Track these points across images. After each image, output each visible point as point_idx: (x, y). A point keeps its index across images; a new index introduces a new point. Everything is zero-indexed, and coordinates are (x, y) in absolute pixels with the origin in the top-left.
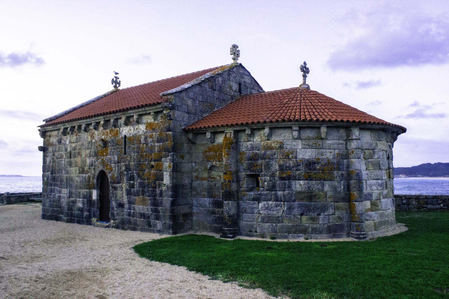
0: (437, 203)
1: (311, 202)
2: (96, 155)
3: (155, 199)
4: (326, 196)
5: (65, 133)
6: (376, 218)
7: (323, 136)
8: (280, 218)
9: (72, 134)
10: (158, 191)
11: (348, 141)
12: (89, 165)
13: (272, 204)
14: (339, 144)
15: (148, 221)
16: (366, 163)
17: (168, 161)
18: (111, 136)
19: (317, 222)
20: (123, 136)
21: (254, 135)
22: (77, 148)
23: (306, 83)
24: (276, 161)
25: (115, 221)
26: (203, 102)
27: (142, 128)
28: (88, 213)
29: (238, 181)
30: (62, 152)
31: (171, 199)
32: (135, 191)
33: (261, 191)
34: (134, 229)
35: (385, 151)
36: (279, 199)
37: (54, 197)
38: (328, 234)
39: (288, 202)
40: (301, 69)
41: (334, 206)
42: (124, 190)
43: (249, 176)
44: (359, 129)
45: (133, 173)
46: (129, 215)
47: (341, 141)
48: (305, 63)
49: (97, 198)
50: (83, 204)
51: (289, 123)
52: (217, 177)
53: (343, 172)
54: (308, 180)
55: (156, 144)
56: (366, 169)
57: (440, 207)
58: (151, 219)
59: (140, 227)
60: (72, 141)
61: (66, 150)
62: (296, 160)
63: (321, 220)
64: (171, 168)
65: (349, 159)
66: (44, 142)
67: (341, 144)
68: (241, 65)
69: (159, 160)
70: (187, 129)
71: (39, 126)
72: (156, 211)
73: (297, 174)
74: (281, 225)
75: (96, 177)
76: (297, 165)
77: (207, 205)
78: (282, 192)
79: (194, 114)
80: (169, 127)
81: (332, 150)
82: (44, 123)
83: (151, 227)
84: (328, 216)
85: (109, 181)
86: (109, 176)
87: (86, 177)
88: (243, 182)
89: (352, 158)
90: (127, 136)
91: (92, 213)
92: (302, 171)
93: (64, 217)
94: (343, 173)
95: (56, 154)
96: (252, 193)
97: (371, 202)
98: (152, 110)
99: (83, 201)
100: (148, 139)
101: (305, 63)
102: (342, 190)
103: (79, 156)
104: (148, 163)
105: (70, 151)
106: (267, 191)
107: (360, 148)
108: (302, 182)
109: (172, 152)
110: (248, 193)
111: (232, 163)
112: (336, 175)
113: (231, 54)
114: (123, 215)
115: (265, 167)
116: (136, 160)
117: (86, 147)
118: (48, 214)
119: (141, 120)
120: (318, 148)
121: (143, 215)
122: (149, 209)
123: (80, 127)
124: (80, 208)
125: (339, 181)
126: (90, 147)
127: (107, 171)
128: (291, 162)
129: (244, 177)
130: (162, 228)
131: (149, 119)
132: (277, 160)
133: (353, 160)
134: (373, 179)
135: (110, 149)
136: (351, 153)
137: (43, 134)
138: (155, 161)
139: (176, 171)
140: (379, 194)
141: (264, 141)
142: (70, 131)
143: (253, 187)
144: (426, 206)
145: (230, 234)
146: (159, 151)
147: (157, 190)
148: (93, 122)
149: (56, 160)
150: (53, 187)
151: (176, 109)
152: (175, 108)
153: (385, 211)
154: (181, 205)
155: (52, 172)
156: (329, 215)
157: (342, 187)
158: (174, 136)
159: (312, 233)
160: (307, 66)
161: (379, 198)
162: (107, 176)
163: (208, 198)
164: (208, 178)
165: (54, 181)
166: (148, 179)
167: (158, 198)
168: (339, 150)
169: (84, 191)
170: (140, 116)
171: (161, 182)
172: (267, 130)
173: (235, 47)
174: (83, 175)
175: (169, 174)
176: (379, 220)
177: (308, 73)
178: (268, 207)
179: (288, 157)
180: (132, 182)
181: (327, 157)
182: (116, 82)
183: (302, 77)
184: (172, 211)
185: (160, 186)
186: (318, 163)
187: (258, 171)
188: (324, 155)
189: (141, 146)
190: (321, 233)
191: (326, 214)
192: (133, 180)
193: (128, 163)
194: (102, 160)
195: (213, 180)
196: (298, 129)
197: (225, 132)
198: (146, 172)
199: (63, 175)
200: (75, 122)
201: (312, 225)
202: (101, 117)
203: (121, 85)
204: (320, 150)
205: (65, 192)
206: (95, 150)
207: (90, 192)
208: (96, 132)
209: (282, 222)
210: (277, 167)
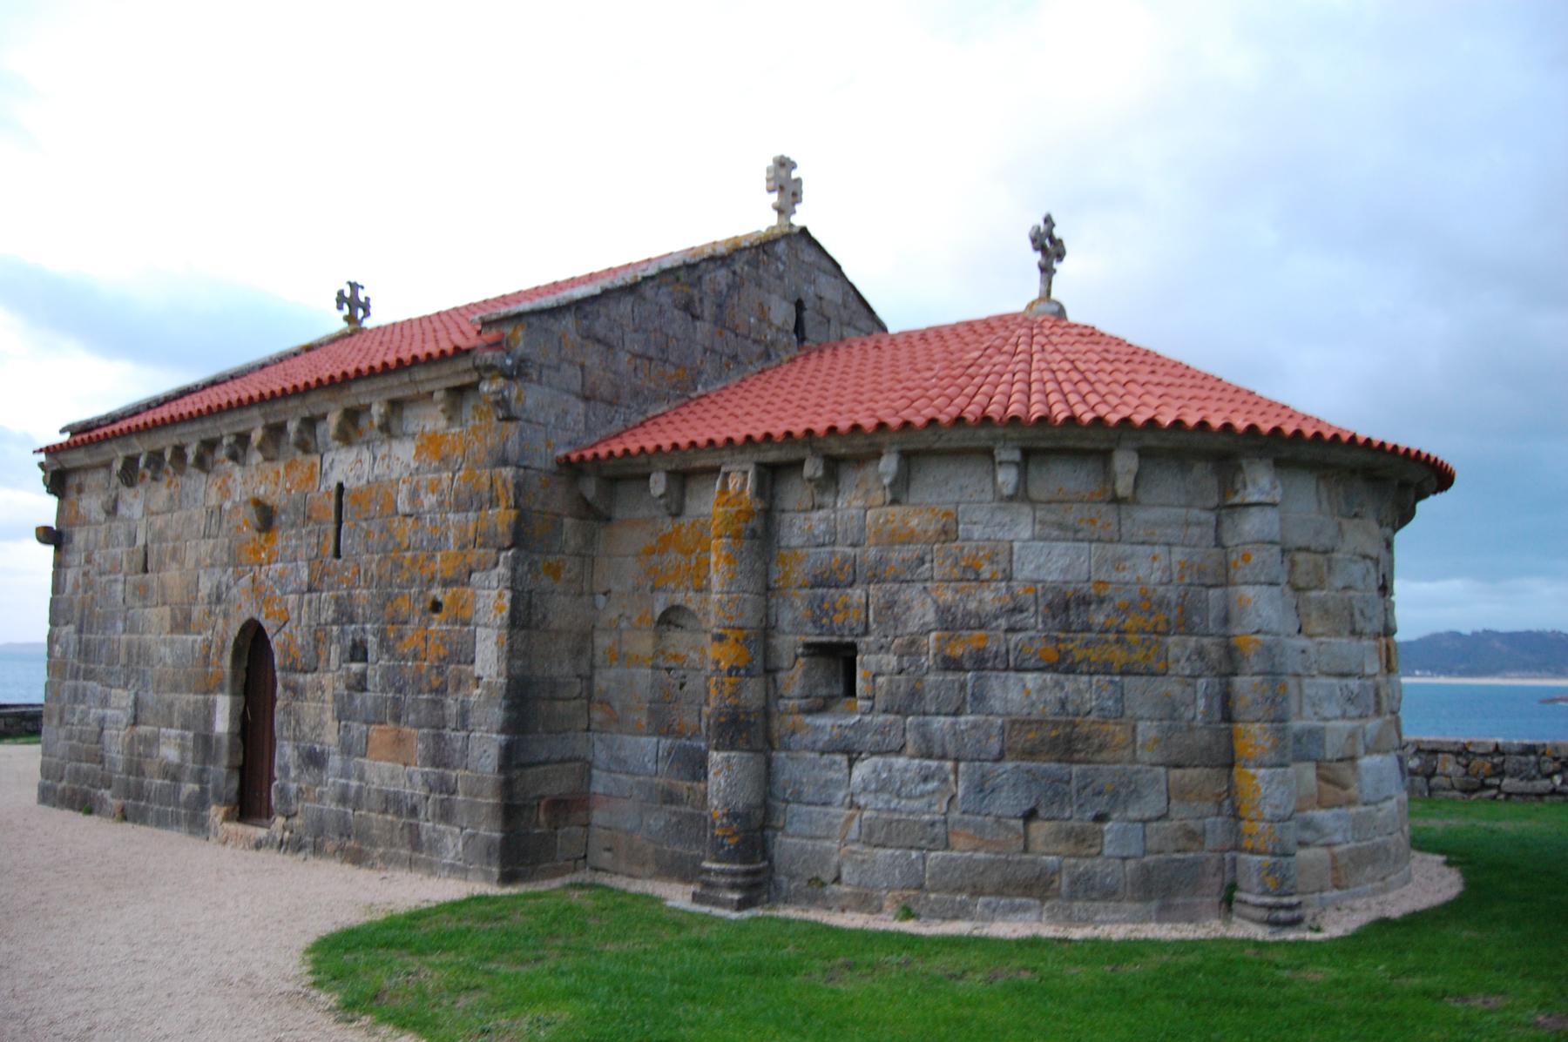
0: (1539, 771)
1: (1072, 762)
2: (234, 560)
3: (439, 738)
4: (1134, 741)
5: (129, 474)
6: (1338, 838)
7: (1123, 486)
8: (936, 830)
9: (154, 479)
10: (452, 704)
11: (1224, 512)
12: (206, 601)
13: (906, 770)
14: (1188, 524)
15: (411, 825)
16: (1297, 607)
17: (495, 584)
18: (288, 485)
19: (1094, 851)
20: (334, 485)
21: (837, 484)
22: (170, 533)
23: (1054, 295)
24: (925, 588)
25: (290, 821)
26: (650, 359)
27: (404, 453)
28: (197, 787)
29: (770, 671)
30: (118, 551)
31: (502, 738)
32: (369, 703)
33: (863, 714)
34: (357, 858)
35: (1371, 559)
36: (937, 750)
37: (81, 721)
38: (1140, 900)
39: (972, 760)
40: (1034, 240)
41: (1168, 781)
42: (328, 696)
43: (816, 651)
44: (1270, 462)
45: (363, 630)
46: (343, 799)
47: (1196, 514)
48: (1048, 220)
49: (230, 727)
50: (183, 748)
51: (983, 433)
52: (691, 654)
53: (1206, 641)
54: (1056, 670)
55: (451, 516)
56: (1300, 631)
57: (1551, 787)
58: (422, 815)
59: (381, 850)
60: (154, 508)
61: (132, 540)
62: (1009, 588)
63: (1111, 842)
64: (505, 613)
65: (1230, 589)
66: (60, 510)
67: (1199, 524)
68: (804, 231)
69: (461, 579)
70: (574, 457)
72: (445, 787)
73: (1012, 645)
74: (944, 858)
75: (230, 643)
76: (1011, 605)
77: (650, 765)
78: (950, 720)
79: (610, 403)
80: (504, 449)
81: (1157, 550)
82: (66, 437)
83: (421, 852)
84: (1140, 825)
85: (276, 661)
86: (276, 642)
87: (197, 647)
88: (791, 673)
89: (1246, 583)
90: (346, 485)
91: (210, 786)
92: (1032, 633)
93: (113, 797)
94: (1202, 646)
95: (97, 556)
96: (824, 721)
97: (1318, 768)
98: (437, 382)
99: (183, 738)
100: (422, 496)
101: (1048, 220)
102: (1199, 717)
103: (174, 566)
104: (421, 592)
105: (146, 546)
106: (885, 711)
107: (1278, 539)
108: (1031, 679)
109: (509, 548)
110: (808, 720)
111: (746, 595)
112: (1174, 651)
113: (770, 191)
114: (320, 798)
115: (878, 613)
116: (376, 579)
117: (202, 528)
118: (60, 786)
119: (400, 419)
120: (1099, 540)
121: (391, 802)
122: (418, 779)
123: (179, 452)
124: (168, 764)
125: (1189, 680)
126: (214, 530)
127: (269, 626)
128: (988, 596)
129: (797, 657)
130: (460, 856)
131: (430, 420)
132: (928, 584)
133: (1249, 592)
134: (1329, 674)
135: (285, 539)
136: (1240, 563)
137: (57, 481)
138: (446, 583)
139: (526, 626)
140: (1352, 735)
141: (876, 507)
142: (147, 465)
143: (832, 697)
144: (1496, 781)
145: (733, 887)
146: (463, 547)
147: (450, 701)
148: (225, 432)
149: (97, 578)
150: (81, 683)
151: (535, 377)
152: (526, 375)
153: (1371, 808)
154: (541, 763)
155: (81, 626)
156: (1145, 822)
157: (1201, 703)
158: (518, 486)
159: (1073, 897)
160: (1057, 233)
161: (1348, 753)
162: (268, 642)
163: (648, 735)
164: (655, 656)
165: (86, 661)
166: (415, 657)
167: (453, 734)
168: (1188, 550)
169: (187, 700)
170: (396, 405)
171: (463, 667)
172: (889, 465)
173: (784, 164)
174: (184, 637)
175: (494, 638)
176: (1352, 844)
177: (1060, 256)
178: (889, 780)
179: (978, 574)
180: (356, 667)
181: (1138, 578)
182: (353, 302)
183: (1037, 273)
184: (507, 787)
185: (459, 684)
186: (1101, 601)
187: (851, 630)
189: (396, 525)
190: (1109, 894)
191: (1133, 813)
192: (365, 659)
193: (345, 593)
194: (254, 580)
195: (672, 664)
196: (1016, 456)
197: (723, 469)
198: (409, 629)
199: (116, 637)
200: (163, 434)
201: (1073, 861)
202: (255, 412)
203: (372, 310)
204: (1108, 546)
205: (122, 698)
206: (230, 542)
207: (206, 703)
208: (237, 471)
209: (947, 846)
210: (931, 617)
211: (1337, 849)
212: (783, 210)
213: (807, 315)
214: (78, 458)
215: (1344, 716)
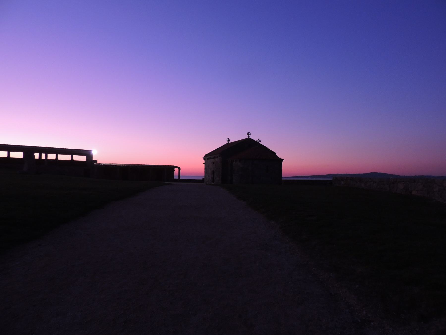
48: (259, 139)
101: (259, 139)
137: (204, 159)
160: (260, 140)
182: (228, 140)
212: (249, 136)
214: (205, 158)
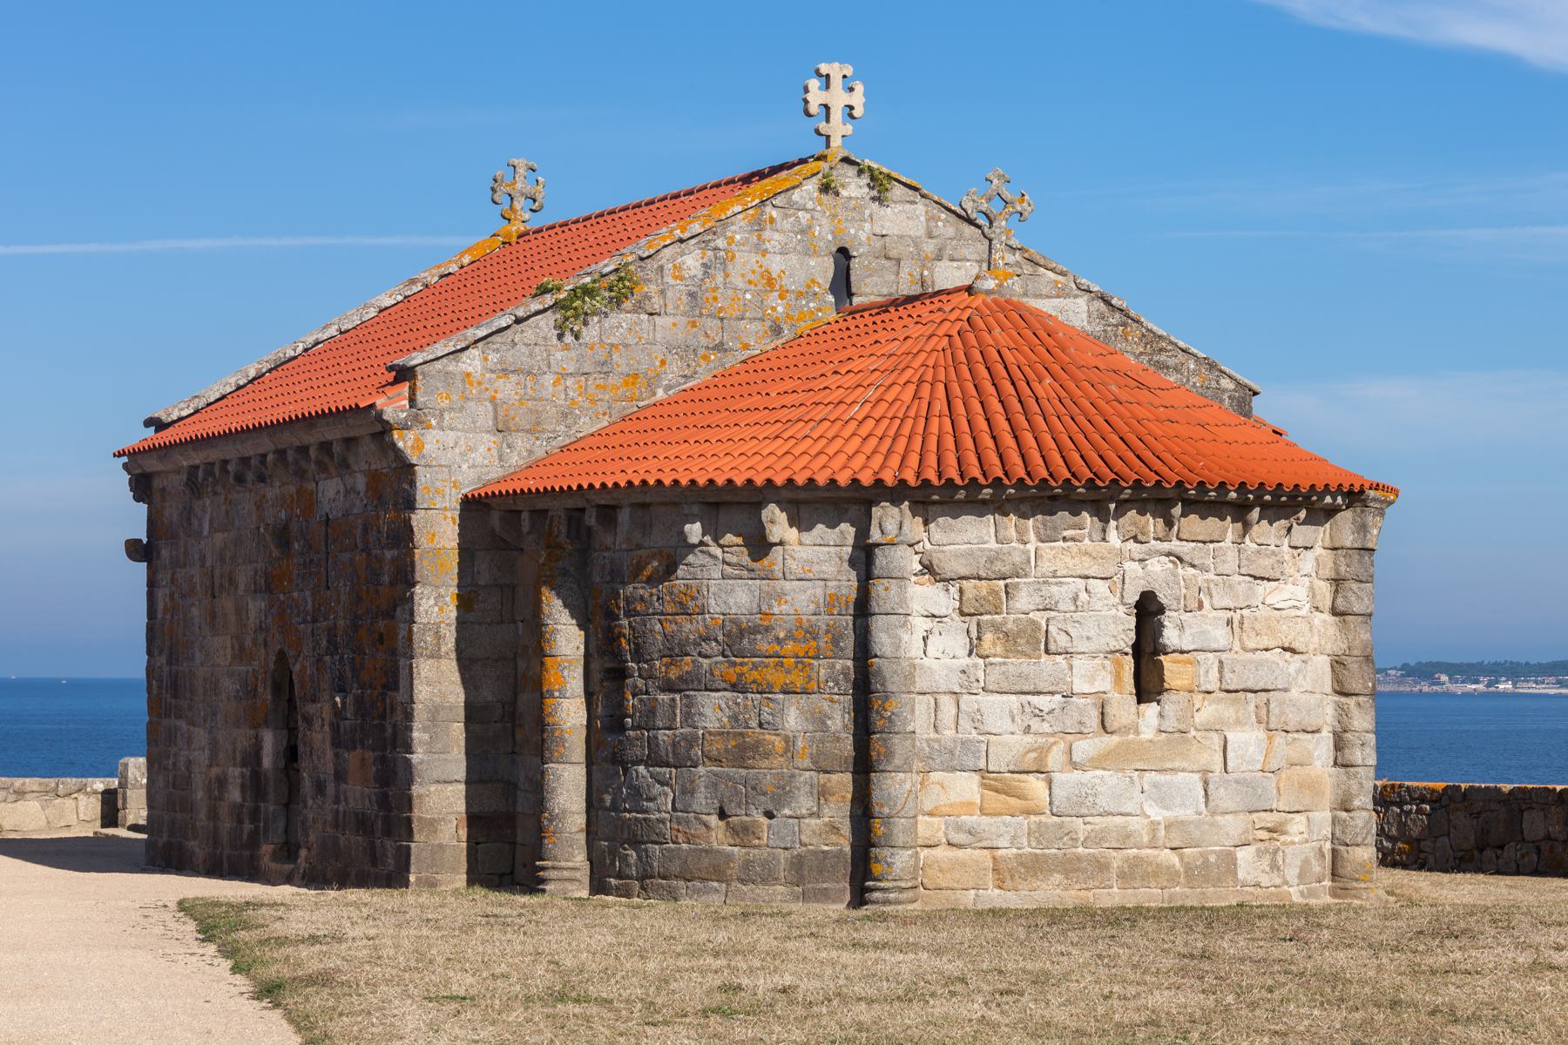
71: (119, 455)
91: (262, 824)
137: (142, 486)
151: (434, 422)
169: (243, 737)
188: (786, 602)
211: (1000, 852)
213: (854, 264)
214: (152, 465)
215: (1027, 730)
